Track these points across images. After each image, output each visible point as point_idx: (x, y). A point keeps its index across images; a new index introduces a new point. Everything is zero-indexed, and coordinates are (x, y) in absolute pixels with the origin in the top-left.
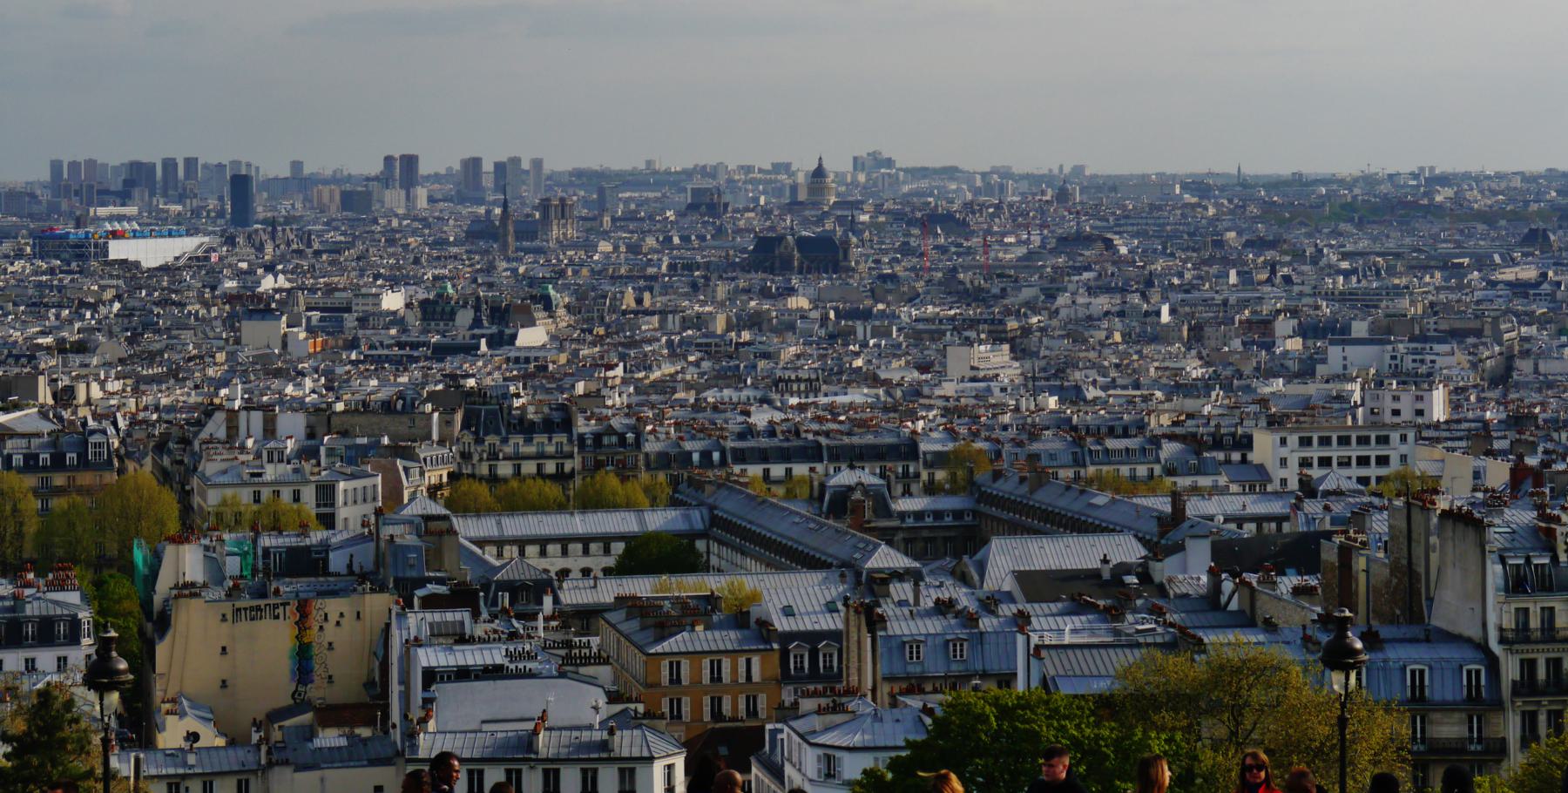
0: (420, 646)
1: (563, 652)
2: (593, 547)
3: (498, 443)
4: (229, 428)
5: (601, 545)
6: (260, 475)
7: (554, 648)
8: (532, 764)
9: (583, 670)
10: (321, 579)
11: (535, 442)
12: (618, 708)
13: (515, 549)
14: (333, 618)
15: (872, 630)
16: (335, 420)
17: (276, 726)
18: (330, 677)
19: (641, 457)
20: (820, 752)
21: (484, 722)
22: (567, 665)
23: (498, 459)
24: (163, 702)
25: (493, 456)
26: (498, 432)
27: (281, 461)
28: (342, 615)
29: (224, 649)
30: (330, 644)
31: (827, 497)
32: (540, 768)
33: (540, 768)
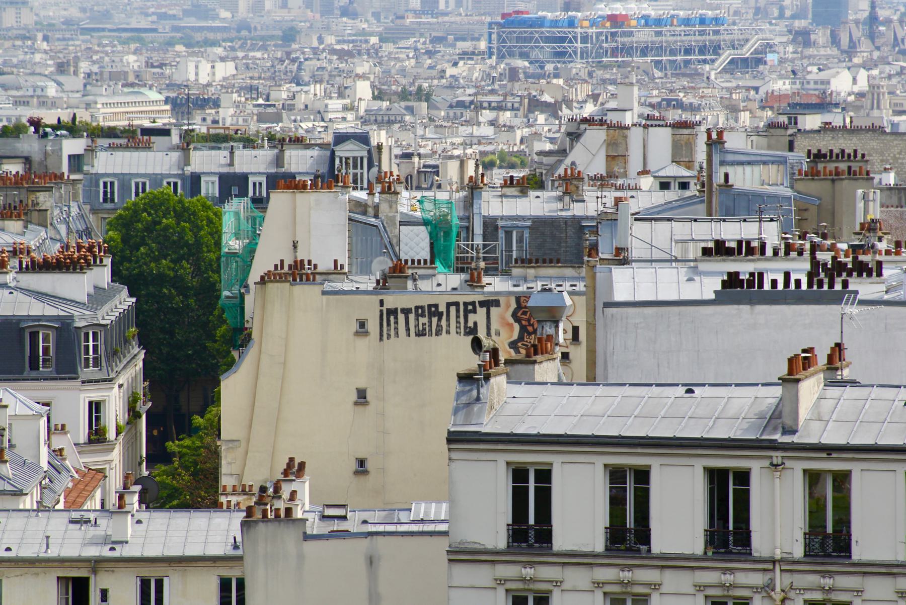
0: (624, 262)
4: (610, 158)
8: (777, 456)
29: (362, 395)
32: (797, 468)
33: (797, 468)
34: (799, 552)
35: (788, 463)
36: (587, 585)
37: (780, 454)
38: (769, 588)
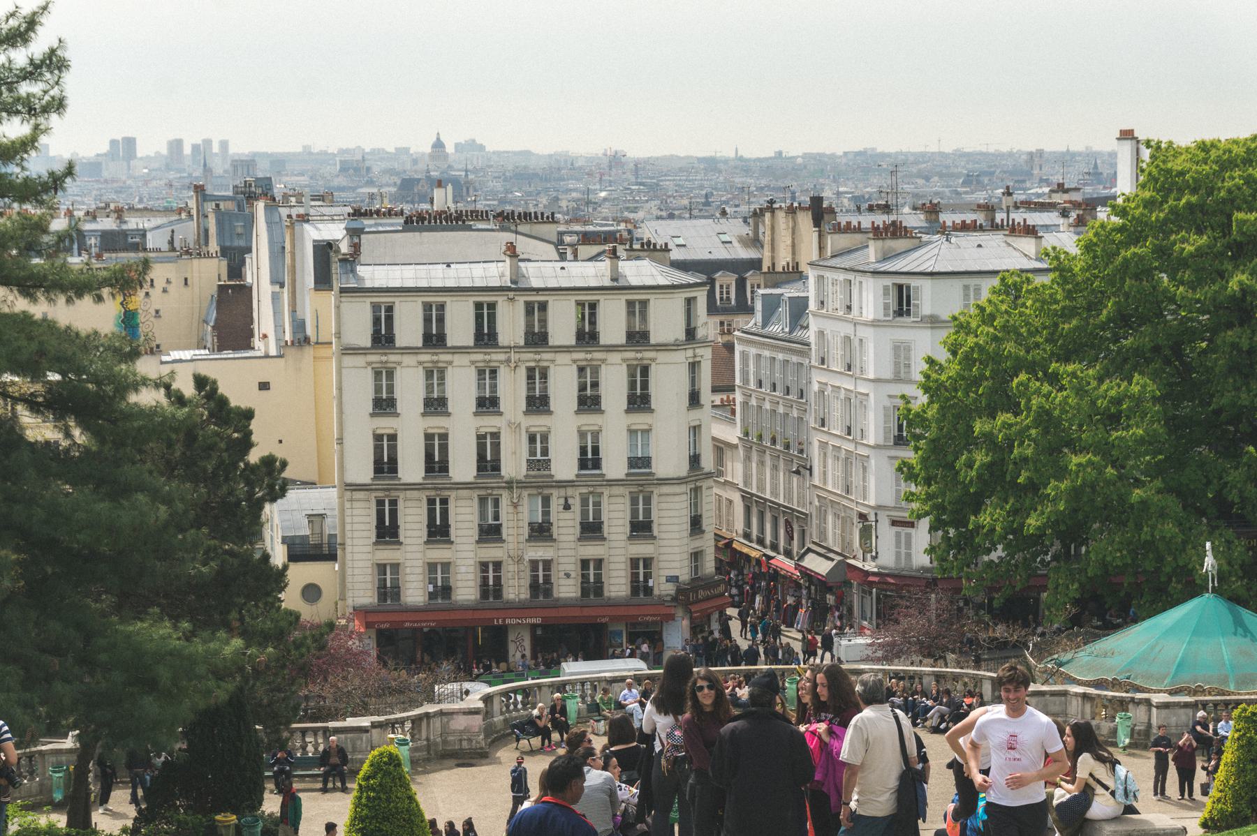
8: (511, 294)
20: (889, 281)
28: (168, 282)
32: (521, 300)
33: (521, 300)
34: (522, 343)
35: (516, 298)
36: (414, 363)
37: (513, 293)
38: (508, 361)
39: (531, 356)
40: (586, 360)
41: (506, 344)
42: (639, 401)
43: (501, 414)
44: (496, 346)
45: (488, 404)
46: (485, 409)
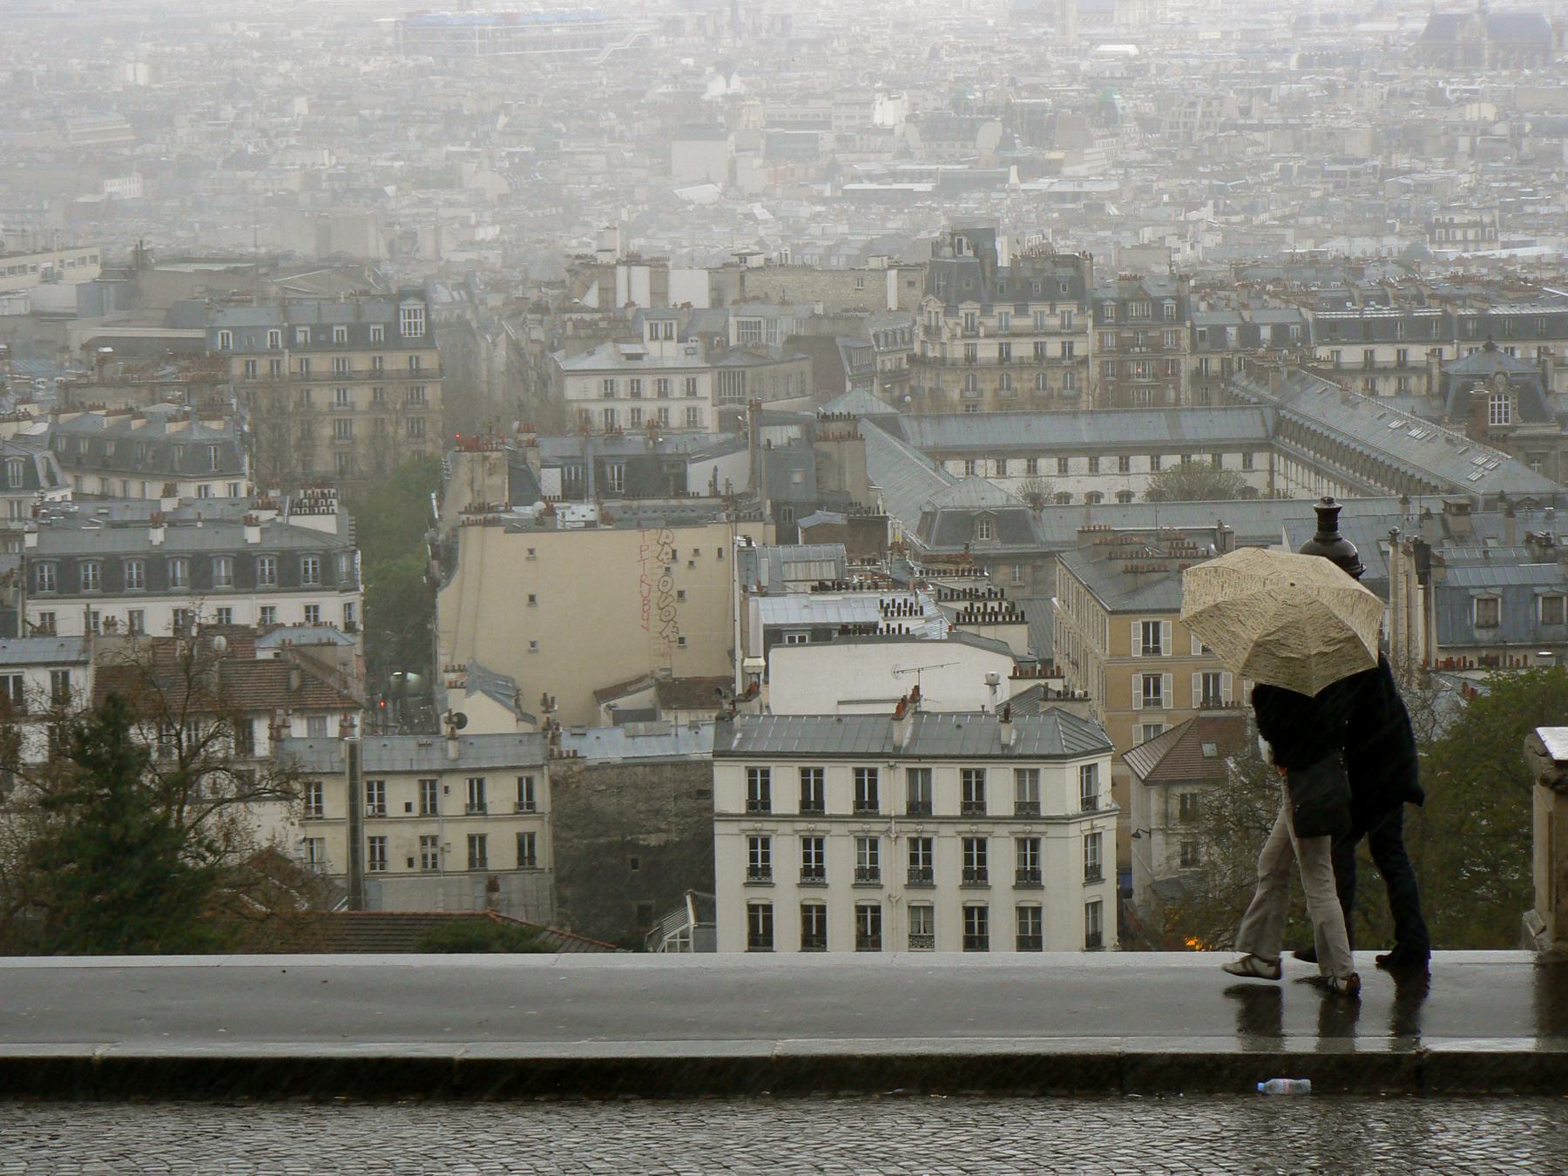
0: (765, 595)
1: (961, 606)
2: (1105, 462)
3: (978, 313)
5: (1116, 459)
6: (639, 357)
7: (952, 600)
8: (892, 762)
9: (987, 632)
10: (673, 502)
11: (1031, 312)
12: (1026, 685)
13: (991, 464)
14: (685, 555)
15: (1423, 579)
16: (751, 280)
17: (604, 705)
18: (682, 640)
19: (1185, 334)
21: (840, 703)
22: (964, 623)
23: (977, 336)
24: (446, 671)
25: (971, 332)
26: (974, 296)
27: (668, 338)
29: (532, 598)
30: (681, 594)
31: (1452, 393)
32: (903, 768)
36: (790, 832)
38: (888, 831)
39: (913, 827)
40: (971, 832)
41: (887, 813)
42: (1029, 877)
43: (880, 887)
44: (876, 815)
45: (868, 875)
46: (864, 881)
